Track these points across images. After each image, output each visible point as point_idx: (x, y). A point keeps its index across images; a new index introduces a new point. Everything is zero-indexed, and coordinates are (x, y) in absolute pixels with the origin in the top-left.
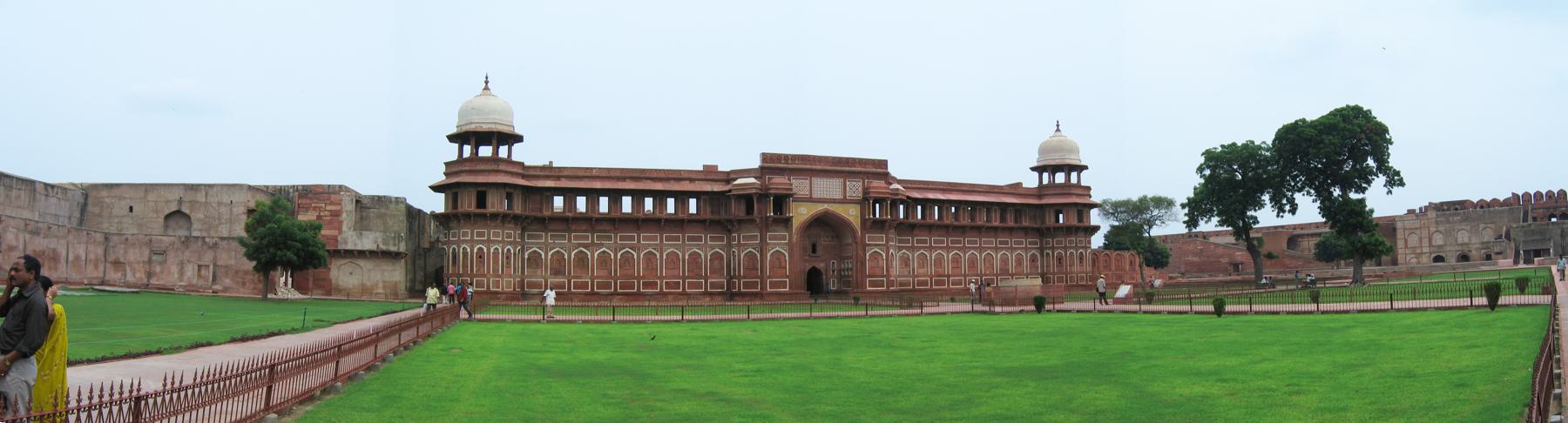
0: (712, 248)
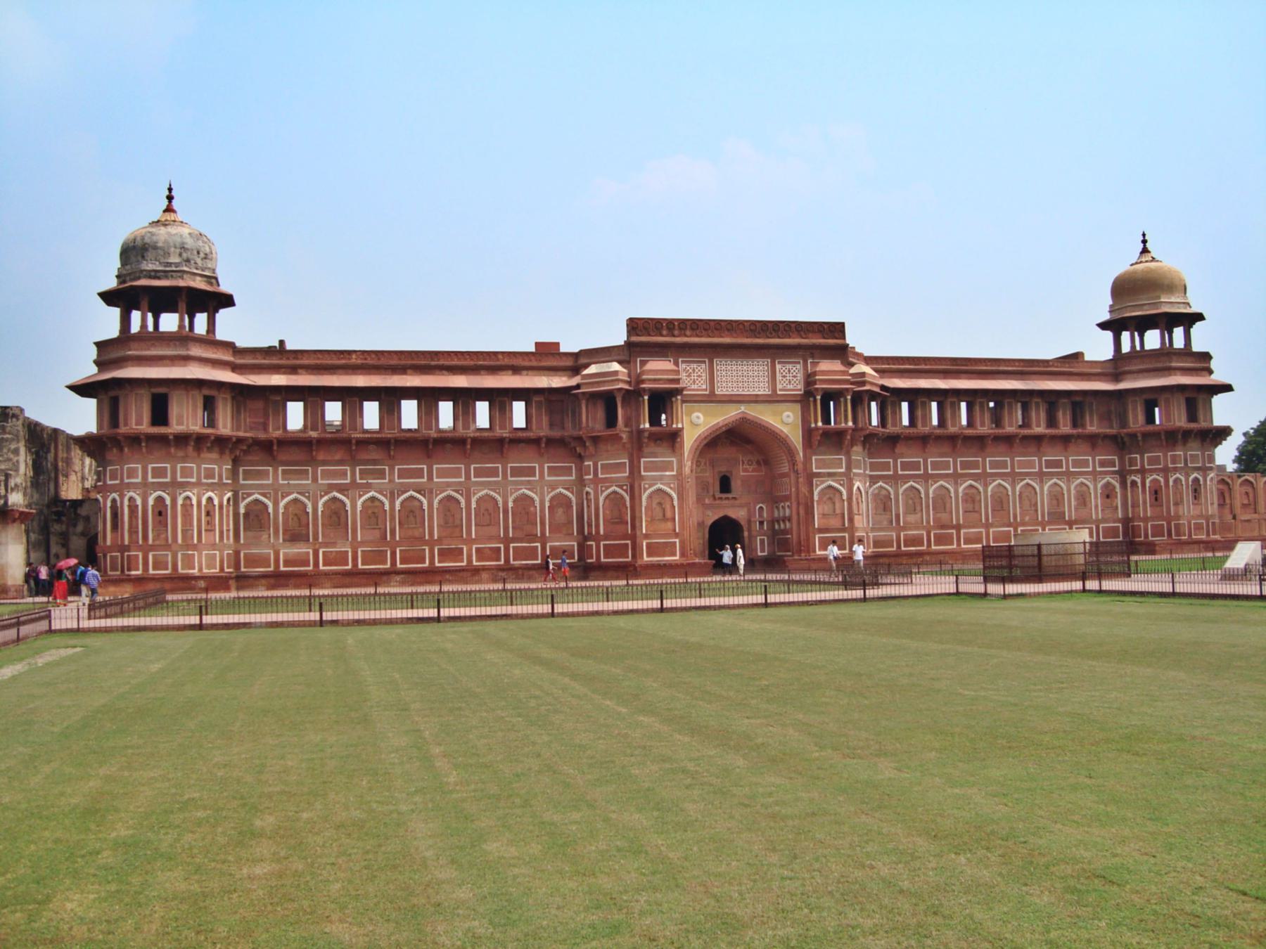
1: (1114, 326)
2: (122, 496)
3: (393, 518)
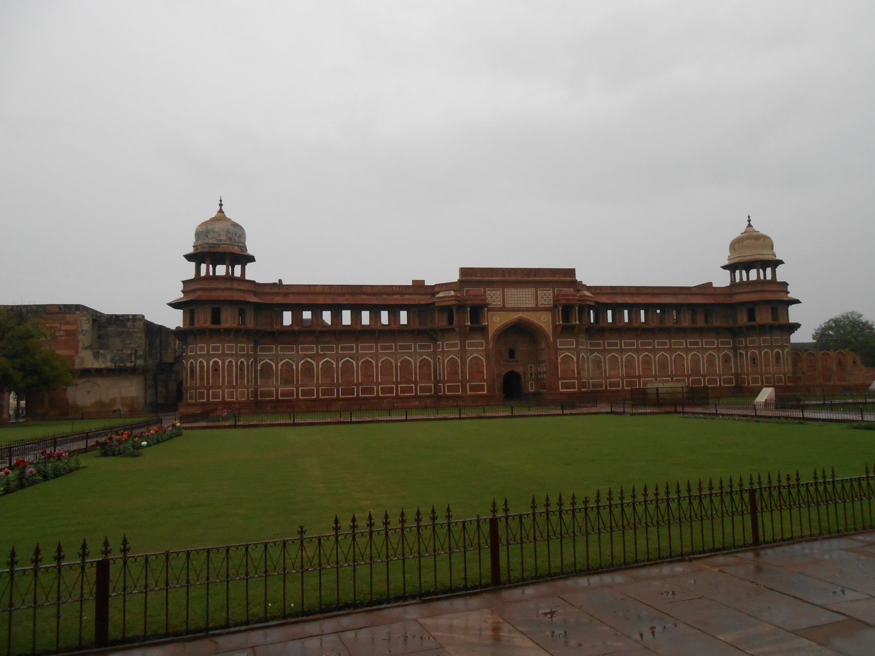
0: (421, 355)
1: (731, 268)
3: (337, 373)
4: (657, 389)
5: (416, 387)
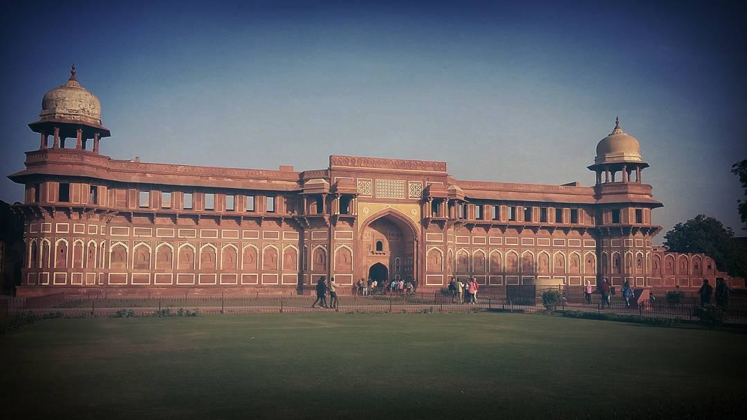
2: (39, 240)
4: (535, 286)
5: (280, 277)
